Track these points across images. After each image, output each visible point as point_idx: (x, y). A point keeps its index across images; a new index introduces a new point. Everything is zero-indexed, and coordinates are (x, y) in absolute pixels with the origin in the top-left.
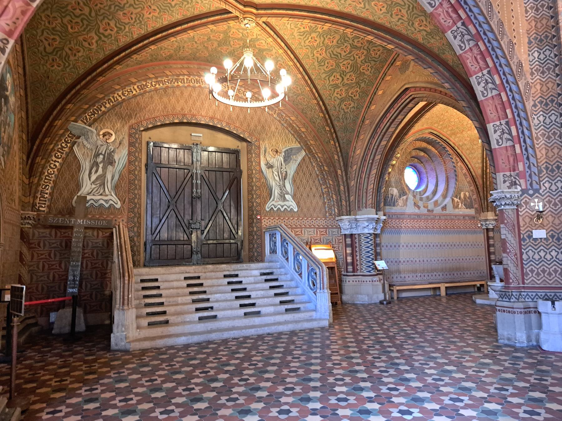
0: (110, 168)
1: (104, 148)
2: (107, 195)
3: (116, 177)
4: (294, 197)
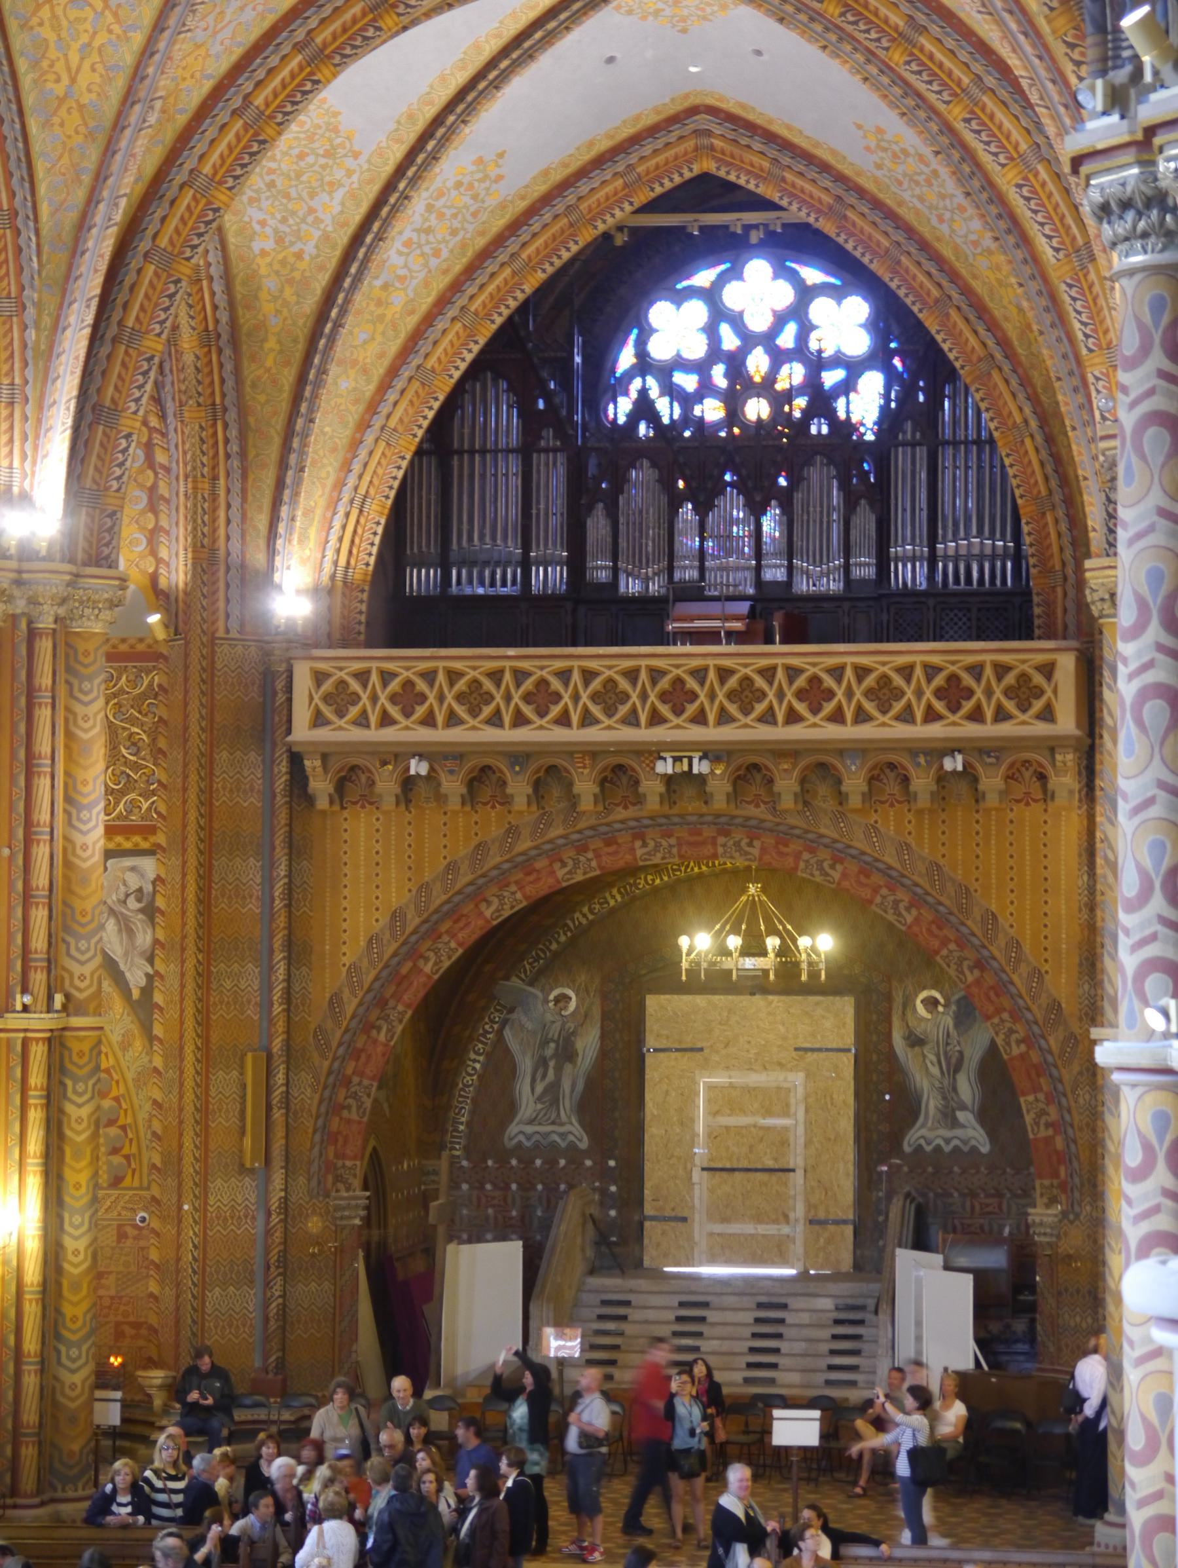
0: (568, 1068)
1: (558, 1025)
2: (562, 1124)
3: (580, 1086)
4: (983, 1116)
